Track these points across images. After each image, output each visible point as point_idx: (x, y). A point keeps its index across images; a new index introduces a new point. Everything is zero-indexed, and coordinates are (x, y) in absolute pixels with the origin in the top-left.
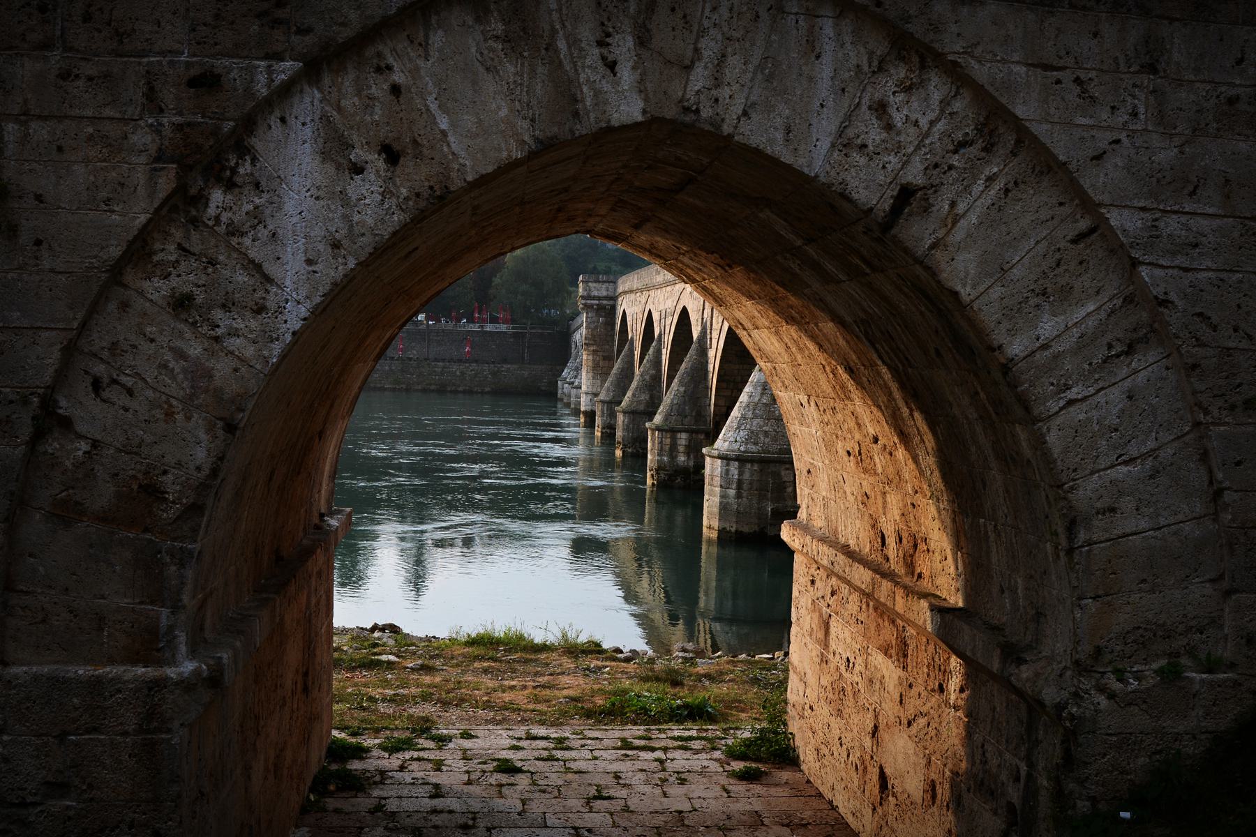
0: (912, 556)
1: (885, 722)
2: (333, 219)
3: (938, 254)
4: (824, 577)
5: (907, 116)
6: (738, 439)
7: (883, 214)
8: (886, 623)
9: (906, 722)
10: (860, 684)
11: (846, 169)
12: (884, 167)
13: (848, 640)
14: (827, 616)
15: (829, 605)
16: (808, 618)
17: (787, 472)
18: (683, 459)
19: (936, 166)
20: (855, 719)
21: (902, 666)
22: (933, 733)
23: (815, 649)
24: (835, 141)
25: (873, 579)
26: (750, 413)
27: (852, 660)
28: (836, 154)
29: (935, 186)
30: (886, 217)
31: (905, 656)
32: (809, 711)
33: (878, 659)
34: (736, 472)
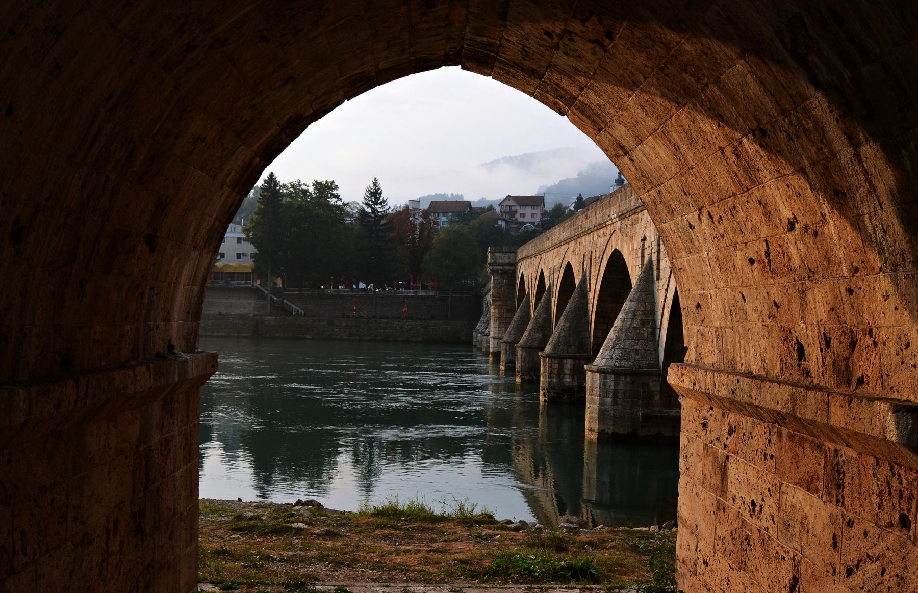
0: (847, 359)
1: (810, 571)
4: (719, 416)
6: (614, 356)
8: (808, 451)
9: (844, 570)
10: (771, 531)
13: (754, 480)
14: (724, 458)
15: (725, 446)
16: (700, 465)
17: (655, 383)
18: (568, 380)
20: (765, 571)
21: (834, 500)
22: (893, 582)
23: (709, 498)
25: (792, 395)
26: (623, 335)
31: (840, 486)
32: (703, 566)
33: (798, 496)
34: (612, 384)
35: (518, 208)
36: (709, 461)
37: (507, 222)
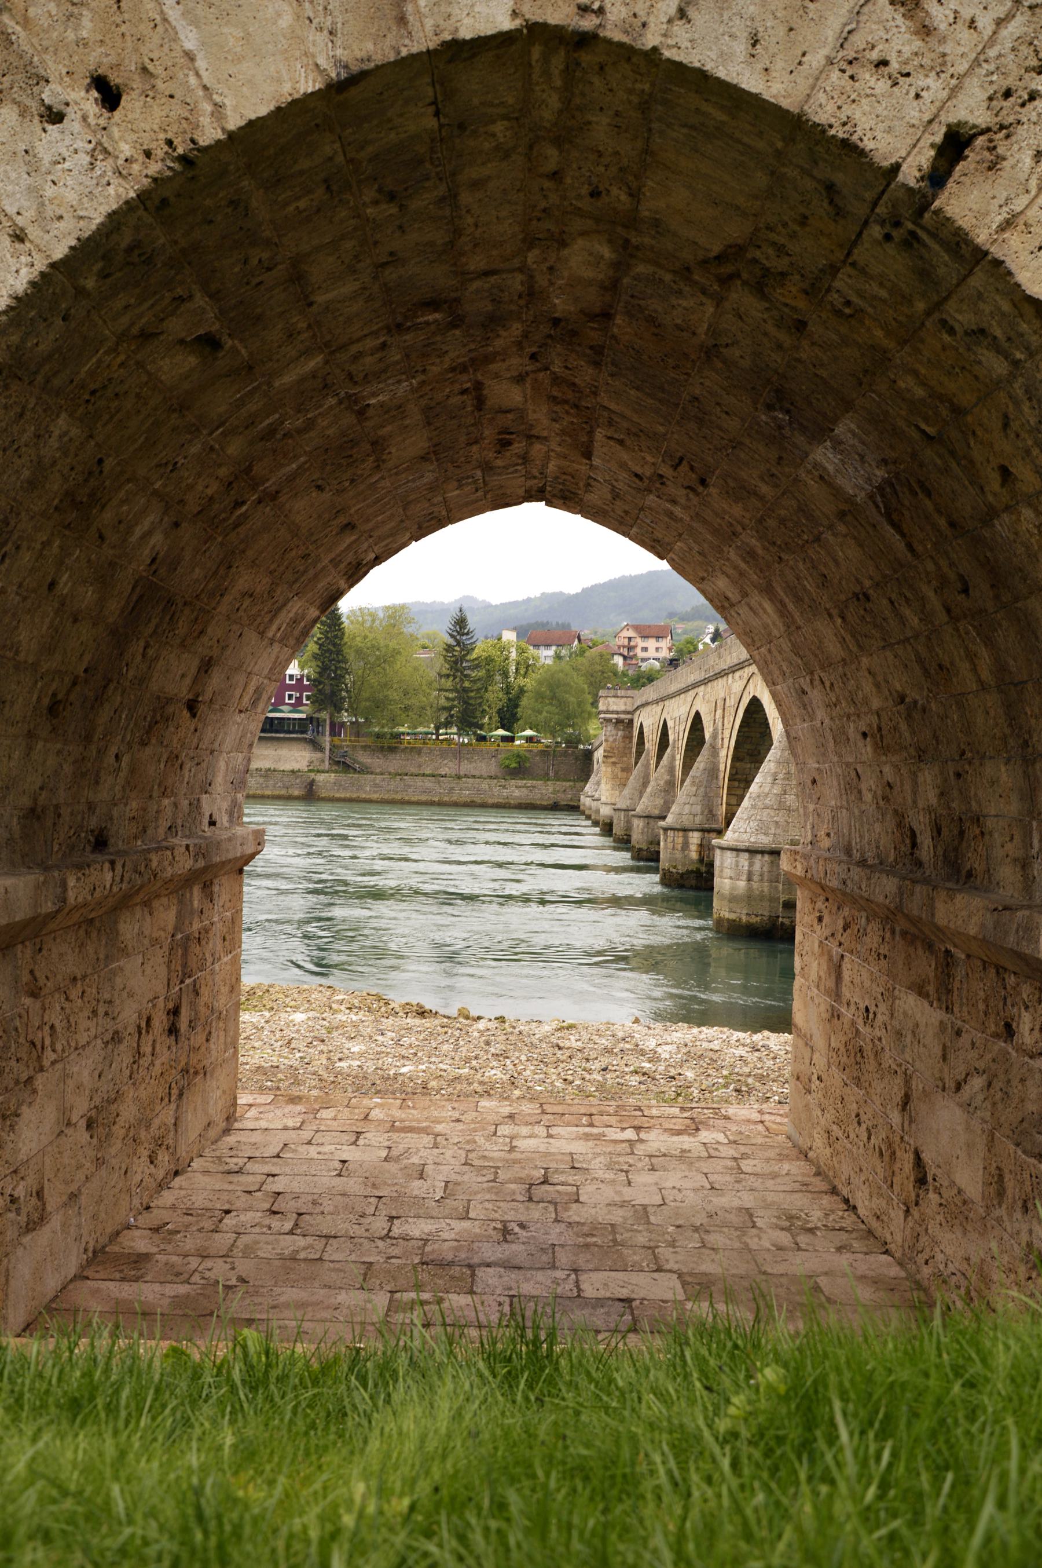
0: (956, 849)
1: (920, 1087)
2: (14, 194)
3: (1014, 239)
4: (834, 911)
5: (956, 12)
7: (918, 175)
8: (920, 952)
9: (953, 1085)
11: (854, 101)
12: (918, 96)
13: (867, 983)
16: (815, 965)
19: (1008, 94)
20: (878, 1086)
23: (824, 1002)
24: (834, 54)
25: (900, 888)
27: (872, 1009)
28: (835, 75)
29: (1006, 128)
30: (922, 178)
31: (949, 991)
33: (909, 1002)
34: (746, 864)
35: (639, 640)
36: (824, 961)
37: (625, 658)
